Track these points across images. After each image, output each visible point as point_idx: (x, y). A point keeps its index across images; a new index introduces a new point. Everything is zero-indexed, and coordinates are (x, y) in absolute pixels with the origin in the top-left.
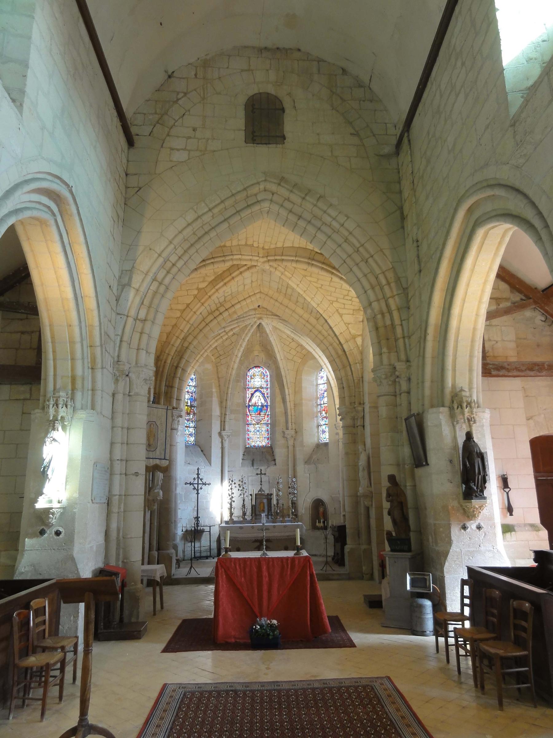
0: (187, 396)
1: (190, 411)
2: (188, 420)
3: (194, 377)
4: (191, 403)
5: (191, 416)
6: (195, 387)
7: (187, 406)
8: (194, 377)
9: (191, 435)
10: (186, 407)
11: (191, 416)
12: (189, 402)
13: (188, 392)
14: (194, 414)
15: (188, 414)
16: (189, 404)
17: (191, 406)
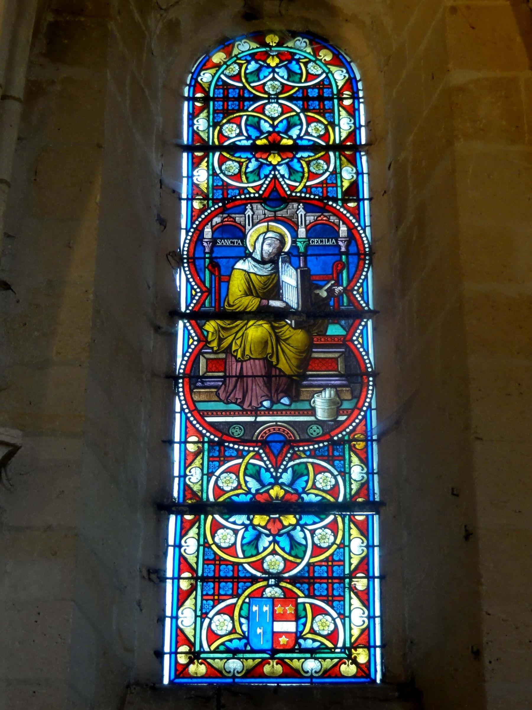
0: (261, 237)
1: (305, 361)
2: (279, 446)
3: (339, 76)
4: (308, 284)
5: (321, 404)
6: (348, 149)
7: (263, 313)
8: (339, 76)
9: (325, 582)
10: (256, 331)
11: (321, 404)
12: (289, 278)
13: (275, 198)
14: (353, 376)
15: (292, 386)
16: (291, 296)
17: (315, 313)
